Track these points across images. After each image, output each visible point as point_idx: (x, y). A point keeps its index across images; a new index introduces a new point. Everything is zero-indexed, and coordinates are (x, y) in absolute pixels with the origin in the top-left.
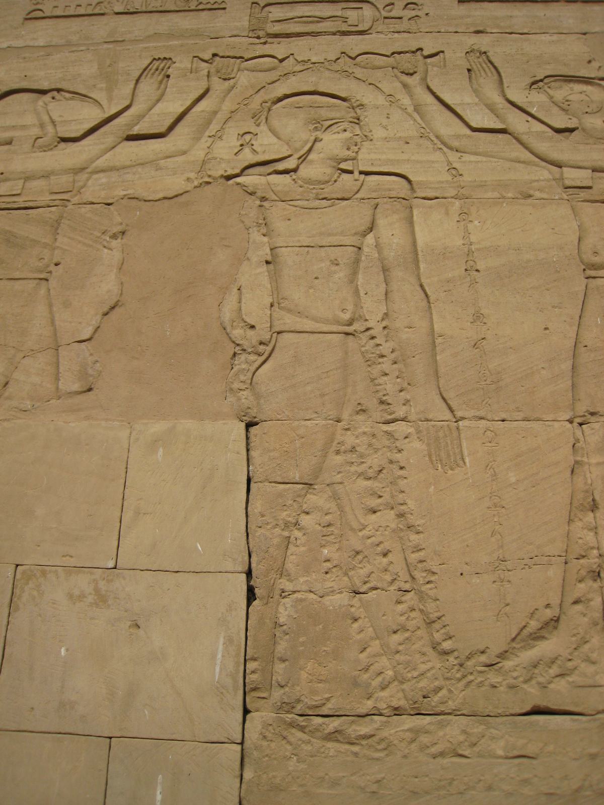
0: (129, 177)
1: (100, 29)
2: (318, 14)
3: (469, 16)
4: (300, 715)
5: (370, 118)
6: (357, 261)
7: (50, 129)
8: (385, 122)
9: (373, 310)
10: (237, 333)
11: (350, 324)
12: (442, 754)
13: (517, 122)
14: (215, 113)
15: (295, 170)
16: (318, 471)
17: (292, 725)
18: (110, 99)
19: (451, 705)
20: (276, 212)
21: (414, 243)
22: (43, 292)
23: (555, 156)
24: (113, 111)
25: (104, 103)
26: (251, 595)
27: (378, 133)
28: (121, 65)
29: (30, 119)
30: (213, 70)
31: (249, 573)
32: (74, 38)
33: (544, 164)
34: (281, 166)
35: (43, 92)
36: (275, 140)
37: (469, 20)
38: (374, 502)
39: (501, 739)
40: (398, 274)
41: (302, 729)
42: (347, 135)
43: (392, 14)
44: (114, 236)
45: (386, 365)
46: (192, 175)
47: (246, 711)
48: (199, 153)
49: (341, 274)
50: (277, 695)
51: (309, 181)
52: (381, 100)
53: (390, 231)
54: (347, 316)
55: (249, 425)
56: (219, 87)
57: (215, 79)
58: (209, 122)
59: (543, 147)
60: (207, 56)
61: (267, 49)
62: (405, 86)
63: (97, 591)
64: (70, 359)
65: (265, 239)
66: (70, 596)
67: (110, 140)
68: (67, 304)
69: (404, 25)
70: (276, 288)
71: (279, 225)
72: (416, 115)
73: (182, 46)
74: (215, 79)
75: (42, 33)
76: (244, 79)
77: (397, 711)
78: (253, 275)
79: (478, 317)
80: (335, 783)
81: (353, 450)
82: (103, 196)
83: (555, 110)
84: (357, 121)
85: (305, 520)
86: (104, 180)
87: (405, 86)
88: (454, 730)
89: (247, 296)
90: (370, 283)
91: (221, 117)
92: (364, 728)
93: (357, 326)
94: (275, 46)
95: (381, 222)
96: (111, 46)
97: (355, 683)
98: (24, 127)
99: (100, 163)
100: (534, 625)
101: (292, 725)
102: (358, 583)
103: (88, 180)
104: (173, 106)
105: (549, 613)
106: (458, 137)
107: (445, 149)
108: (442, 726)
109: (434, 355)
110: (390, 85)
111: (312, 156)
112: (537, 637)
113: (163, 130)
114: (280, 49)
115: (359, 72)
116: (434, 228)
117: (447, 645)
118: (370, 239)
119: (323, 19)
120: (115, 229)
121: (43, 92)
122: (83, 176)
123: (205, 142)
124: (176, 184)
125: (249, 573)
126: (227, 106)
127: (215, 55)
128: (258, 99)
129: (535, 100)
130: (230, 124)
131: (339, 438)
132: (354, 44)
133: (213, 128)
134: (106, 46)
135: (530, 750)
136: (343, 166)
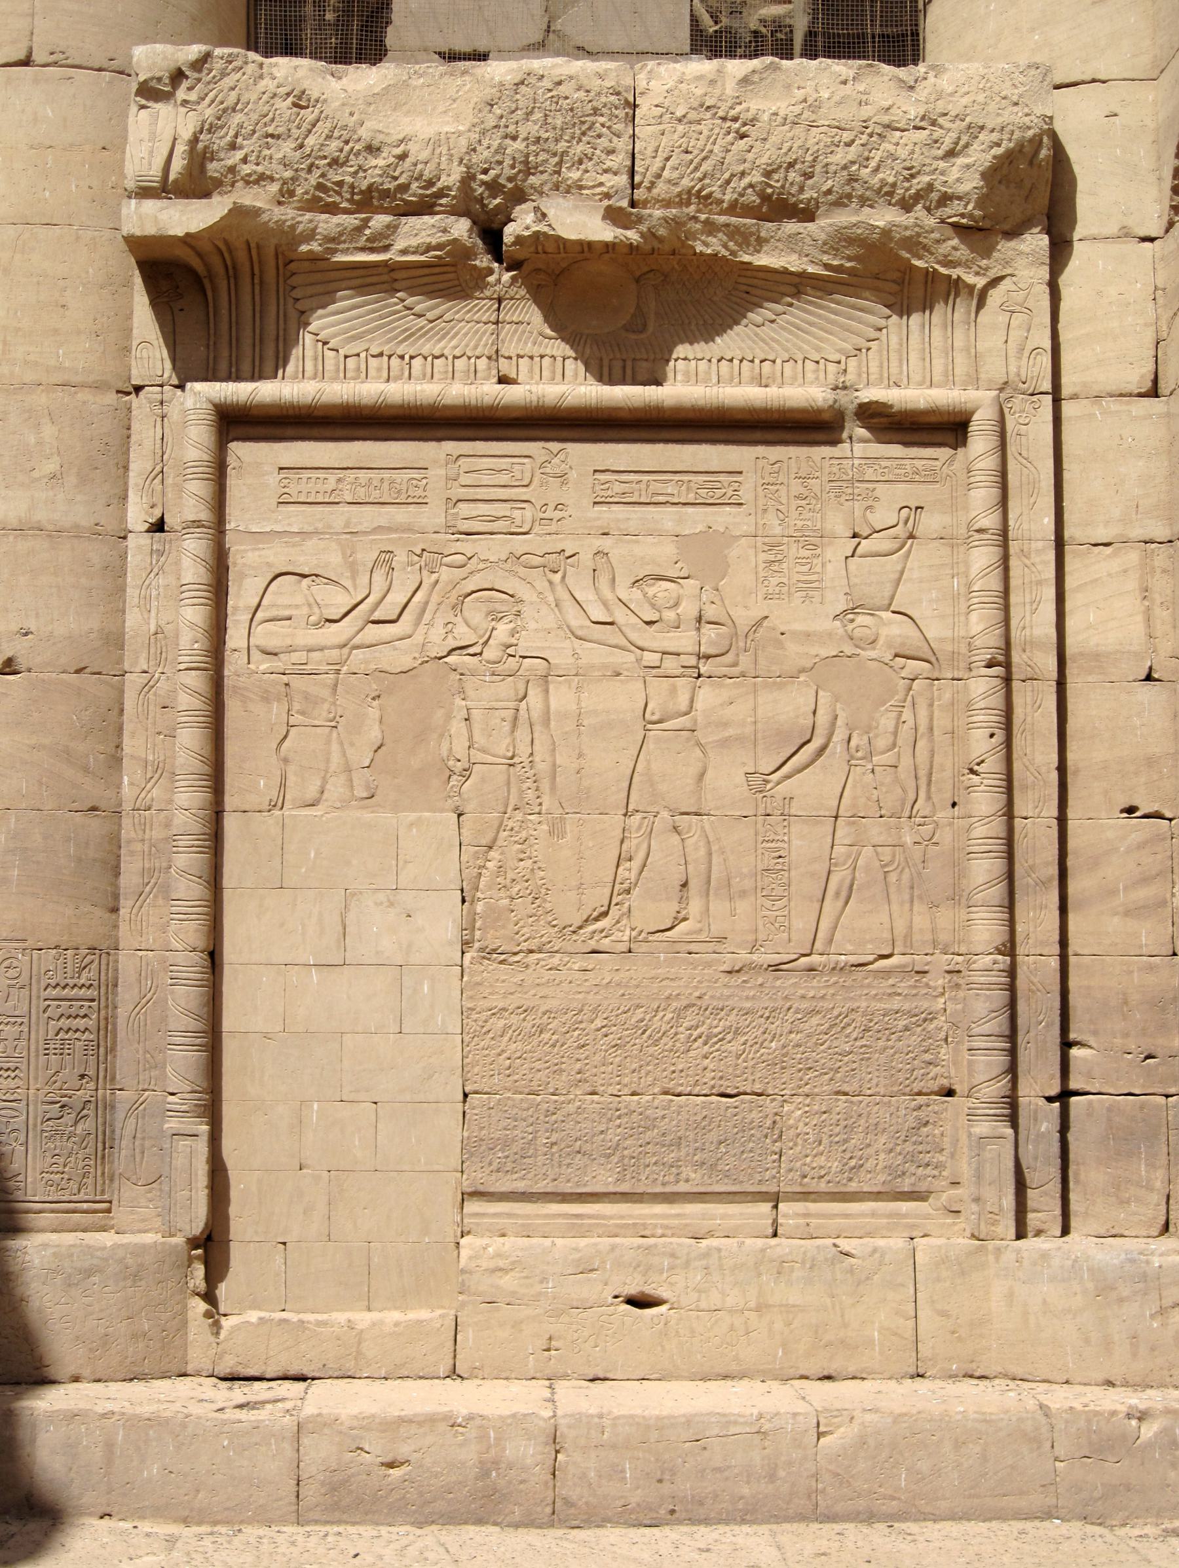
0: (377, 654)
1: (338, 517)
2: (494, 514)
3: (599, 519)
4: (488, 953)
5: (526, 610)
6: (516, 718)
7: (316, 610)
8: (536, 615)
9: (523, 750)
10: (451, 763)
11: (512, 758)
12: (550, 969)
13: (620, 615)
14: (427, 603)
15: (481, 654)
16: (495, 840)
17: (484, 958)
18: (355, 589)
19: (556, 948)
20: (470, 683)
21: (548, 707)
22: (335, 734)
23: (640, 643)
24: (359, 599)
25: (347, 583)
26: (463, 901)
27: (532, 625)
28: (359, 556)
29: (299, 599)
30: (423, 564)
31: (462, 891)
32: (320, 526)
33: (633, 648)
34: (471, 650)
35: (305, 576)
36: (465, 629)
37: (599, 523)
38: (522, 856)
39: (578, 963)
40: (537, 728)
41: (489, 959)
42: (512, 625)
43: (544, 516)
44: (374, 699)
45: (529, 783)
46: (417, 655)
47: (463, 953)
48: (418, 638)
49: (507, 727)
50: (477, 945)
51: (488, 662)
52: (535, 598)
53: (535, 698)
54: (510, 754)
55: (459, 815)
56: (428, 580)
57: (425, 573)
58: (423, 611)
59: (633, 636)
60: (418, 552)
61: (459, 547)
62: (551, 583)
63: (389, 901)
64: (358, 778)
65: (464, 703)
66: (376, 904)
67: (360, 623)
68: (352, 744)
69: (553, 528)
70: (471, 738)
71: (470, 693)
72: (556, 610)
73: (400, 538)
74: (425, 573)
75: (295, 519)
76: (445, 574)
77: (531, 951)
78: (457, 727)
79: (580, 755)
80: (503, 981)
81: (512, 829)
82: (362, 668)
83: (647, 606)
84: (518, 614)
85: (489, 864)
86: (361, 656)
87: (551, 583)
88: (556, 960)
89: (455, 742)
90: (523, 734)
91: (431, 607)
92: (517, 958)
93: (516, 760)
94: (464, 544)
95: (530, 692)
96: (348, 536)
97: (512, 939)
98: (297, 606)
99: (357, 641)
100: (595, 914)
101: (484, 958)
102: (514, 894)
103: (350, 653)
104: (397, 598)
105: (603, 909)
106: (582, 627)
107: (573, 639)
108: (550, 957)
109: (554, 778)
110: (541, 584)
111: (491, 641)
112: (597, 919)
113: (394, 617)
114: (467, 546)
115: (522, 571)
116: (561, 698)
117: (554, 923)
118: (523, 704)
119: (498, 518)
120: (373, 695)
121: (305, 576)
122: (346, 650)
123: (422, 629)
124: (406, 662)
125: (462, 891)
126: (435, 599)
127: (423, 550)
128: (454, 594)
129: (636, 593)
130: (438, 614)
131: (505, 823)
132: (519, 544)
133: (427, 616)
134: (345, 536)
135: (590, 967)
136: (511, 651)
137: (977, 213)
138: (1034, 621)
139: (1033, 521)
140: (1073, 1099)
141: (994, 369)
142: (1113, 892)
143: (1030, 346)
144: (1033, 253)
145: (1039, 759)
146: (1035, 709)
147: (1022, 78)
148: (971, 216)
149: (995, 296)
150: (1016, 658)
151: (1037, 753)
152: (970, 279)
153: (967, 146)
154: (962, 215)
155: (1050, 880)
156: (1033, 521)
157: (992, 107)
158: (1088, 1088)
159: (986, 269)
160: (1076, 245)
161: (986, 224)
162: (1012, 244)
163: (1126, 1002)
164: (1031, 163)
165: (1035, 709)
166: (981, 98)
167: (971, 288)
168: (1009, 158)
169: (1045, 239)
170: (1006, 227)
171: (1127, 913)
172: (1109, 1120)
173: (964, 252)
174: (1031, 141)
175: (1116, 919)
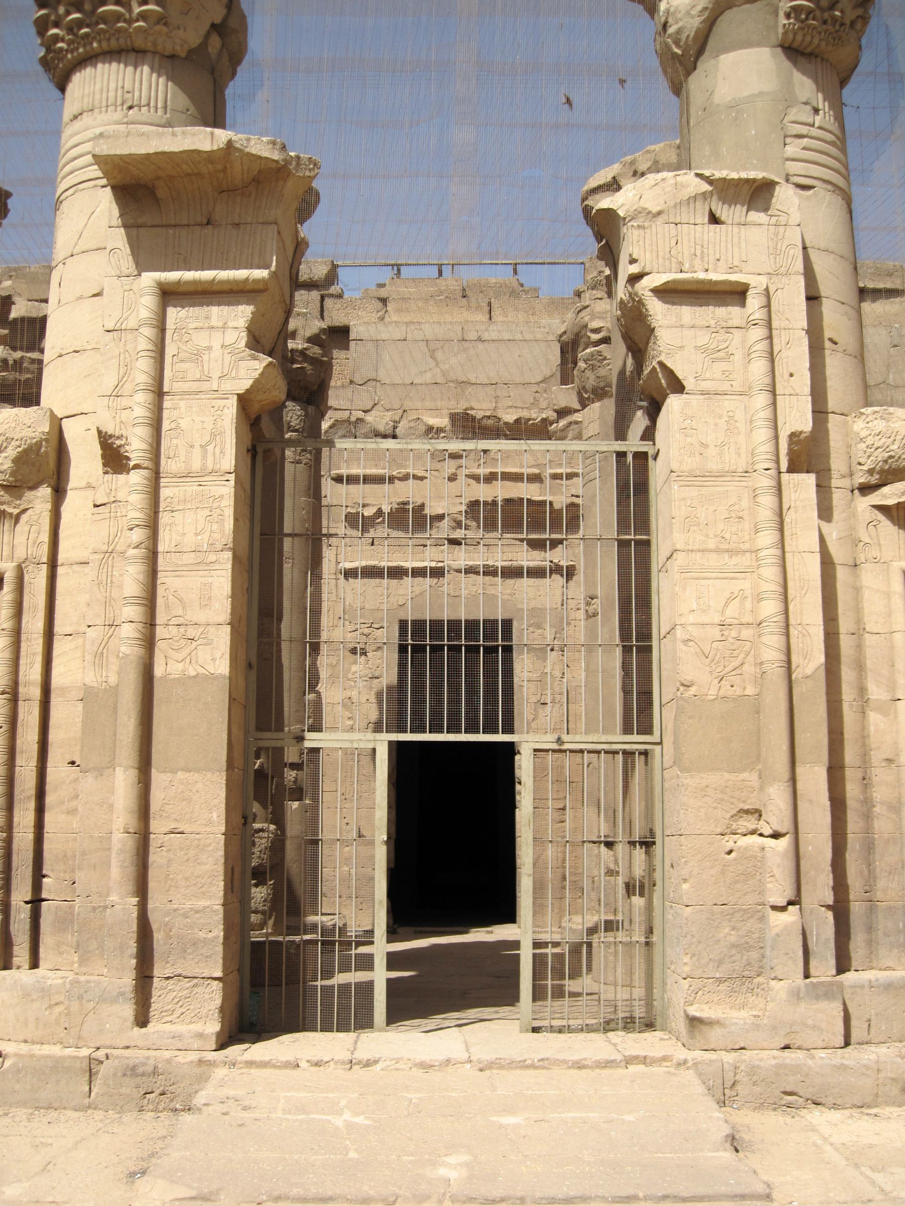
137: (11, 479)
138: (31, 672)
139: (34, 624)
140: (43, 903)
141: (20, 554)
142: (63, 803)
143: (39, 541)
144: (43, 497)
145: (29, 738)
146: (29, 716)
147: (34, 415)
148: (8, 481)
149: (24, 518)
150: (22, 690)
151: (28, 737)
152: (10, 510)
153: (6, 447)
154: (4, 480)
155: (31, 796)
156: (34, 624)
157: (18, 429)
158: (49, 898)
159: (19, 505)
160: (69, 492)
161: (18, 484)
162: (33, 493)
163: (66, 856)
164: (37, 455)
165: (29, 716)
166: (13, 425)
167: (11, 515)
168: (26, 452)
169: (49, 490)
170: (30, 485)
171: (68, 813)
172: (56, 913)
173: (7, 498)
174: (36, 443)
175: (63, 816)
